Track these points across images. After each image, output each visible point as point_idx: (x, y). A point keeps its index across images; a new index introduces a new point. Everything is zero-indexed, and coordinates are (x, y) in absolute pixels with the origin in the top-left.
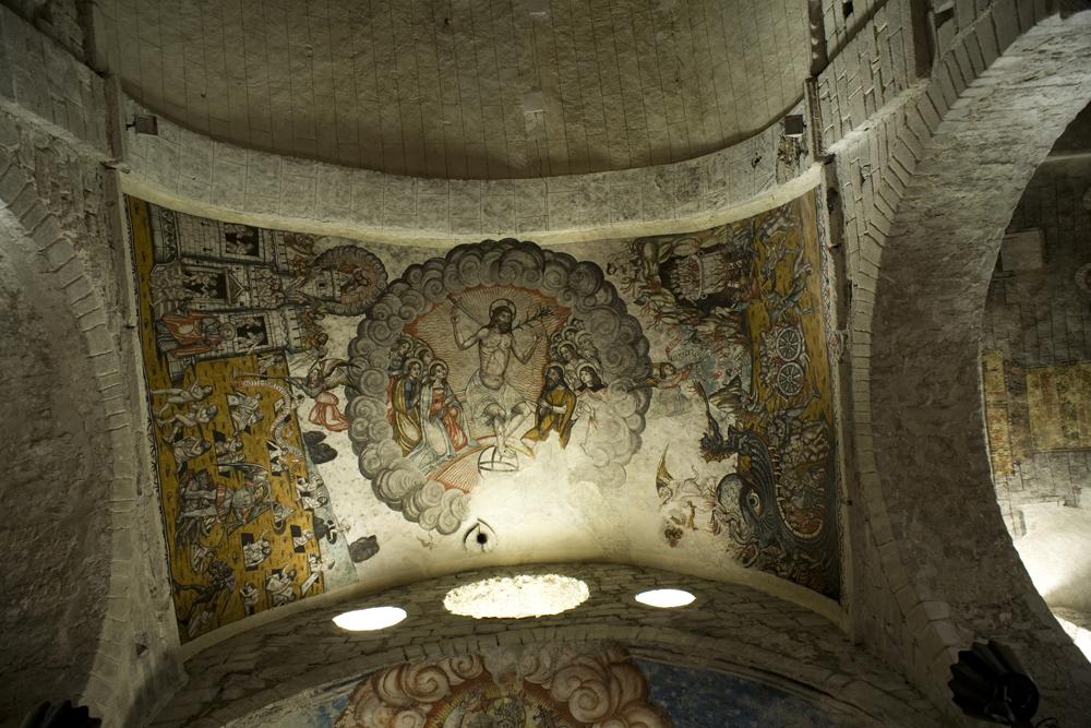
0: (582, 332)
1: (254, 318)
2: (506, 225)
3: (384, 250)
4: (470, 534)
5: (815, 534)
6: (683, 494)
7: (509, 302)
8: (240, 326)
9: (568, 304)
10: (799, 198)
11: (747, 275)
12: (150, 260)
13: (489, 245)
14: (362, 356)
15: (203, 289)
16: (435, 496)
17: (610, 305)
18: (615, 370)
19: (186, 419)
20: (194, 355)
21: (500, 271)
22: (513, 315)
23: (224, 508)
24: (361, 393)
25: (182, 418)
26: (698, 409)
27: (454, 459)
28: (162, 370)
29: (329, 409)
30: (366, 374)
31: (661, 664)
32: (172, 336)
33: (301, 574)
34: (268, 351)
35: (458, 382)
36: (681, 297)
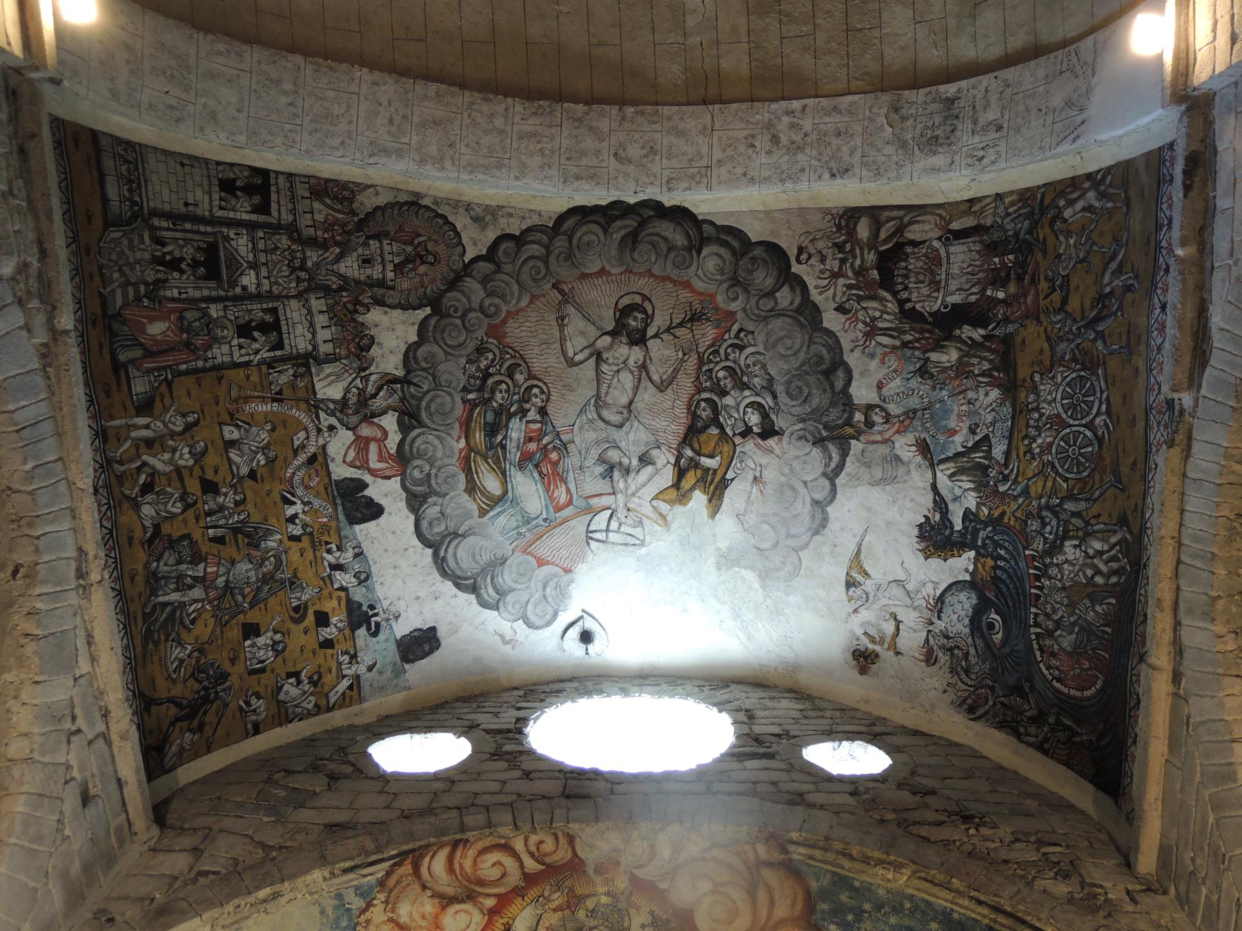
0: (751, 350)
1: (264, 311)
2: (646, 180)
3: (461, 210)
4: (571, 630)
5: (1088, 693)
6: (884, 601)
7: (645, 298)
8: (242, 321)
9: (735, 306)
10: (1128, 161)
11: (1020, 279)
12: (98, 223)
13: (617, 210)
14: (424, 369)
15: (183, 266)
16: (523, 575)
17: (796, 311)
18: (797, 410)
19: (159, 462)
20: (170, 367)
21: (633, 249)
22: (648, 319)
23: (216, 588)
24: (421, 424)
25: (151, 460)
26: (919, 478)
27: (551, 524)
28: (119, 391)
29: (373, 447)
30: (429, 397)
31: (834, 874)
32: (136, 339)
33: (328, 679)
34: (283, 360)
35: (562, 415)
36: (908, 306)
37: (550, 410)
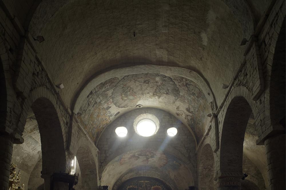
37: (134, 90)
